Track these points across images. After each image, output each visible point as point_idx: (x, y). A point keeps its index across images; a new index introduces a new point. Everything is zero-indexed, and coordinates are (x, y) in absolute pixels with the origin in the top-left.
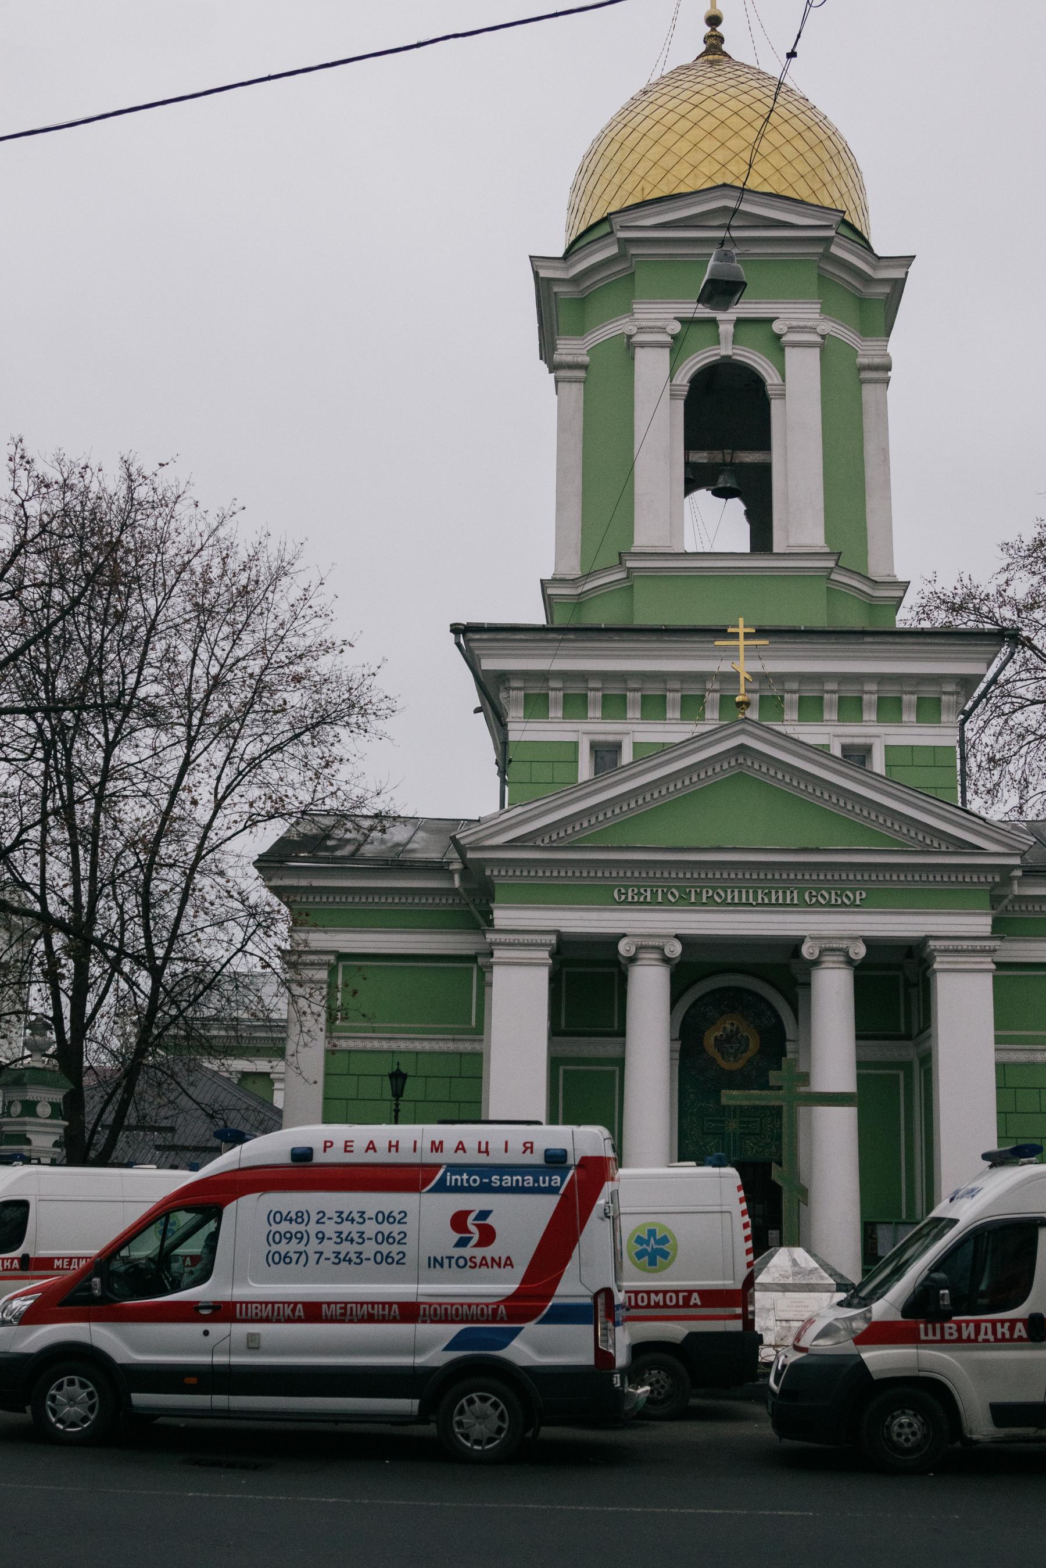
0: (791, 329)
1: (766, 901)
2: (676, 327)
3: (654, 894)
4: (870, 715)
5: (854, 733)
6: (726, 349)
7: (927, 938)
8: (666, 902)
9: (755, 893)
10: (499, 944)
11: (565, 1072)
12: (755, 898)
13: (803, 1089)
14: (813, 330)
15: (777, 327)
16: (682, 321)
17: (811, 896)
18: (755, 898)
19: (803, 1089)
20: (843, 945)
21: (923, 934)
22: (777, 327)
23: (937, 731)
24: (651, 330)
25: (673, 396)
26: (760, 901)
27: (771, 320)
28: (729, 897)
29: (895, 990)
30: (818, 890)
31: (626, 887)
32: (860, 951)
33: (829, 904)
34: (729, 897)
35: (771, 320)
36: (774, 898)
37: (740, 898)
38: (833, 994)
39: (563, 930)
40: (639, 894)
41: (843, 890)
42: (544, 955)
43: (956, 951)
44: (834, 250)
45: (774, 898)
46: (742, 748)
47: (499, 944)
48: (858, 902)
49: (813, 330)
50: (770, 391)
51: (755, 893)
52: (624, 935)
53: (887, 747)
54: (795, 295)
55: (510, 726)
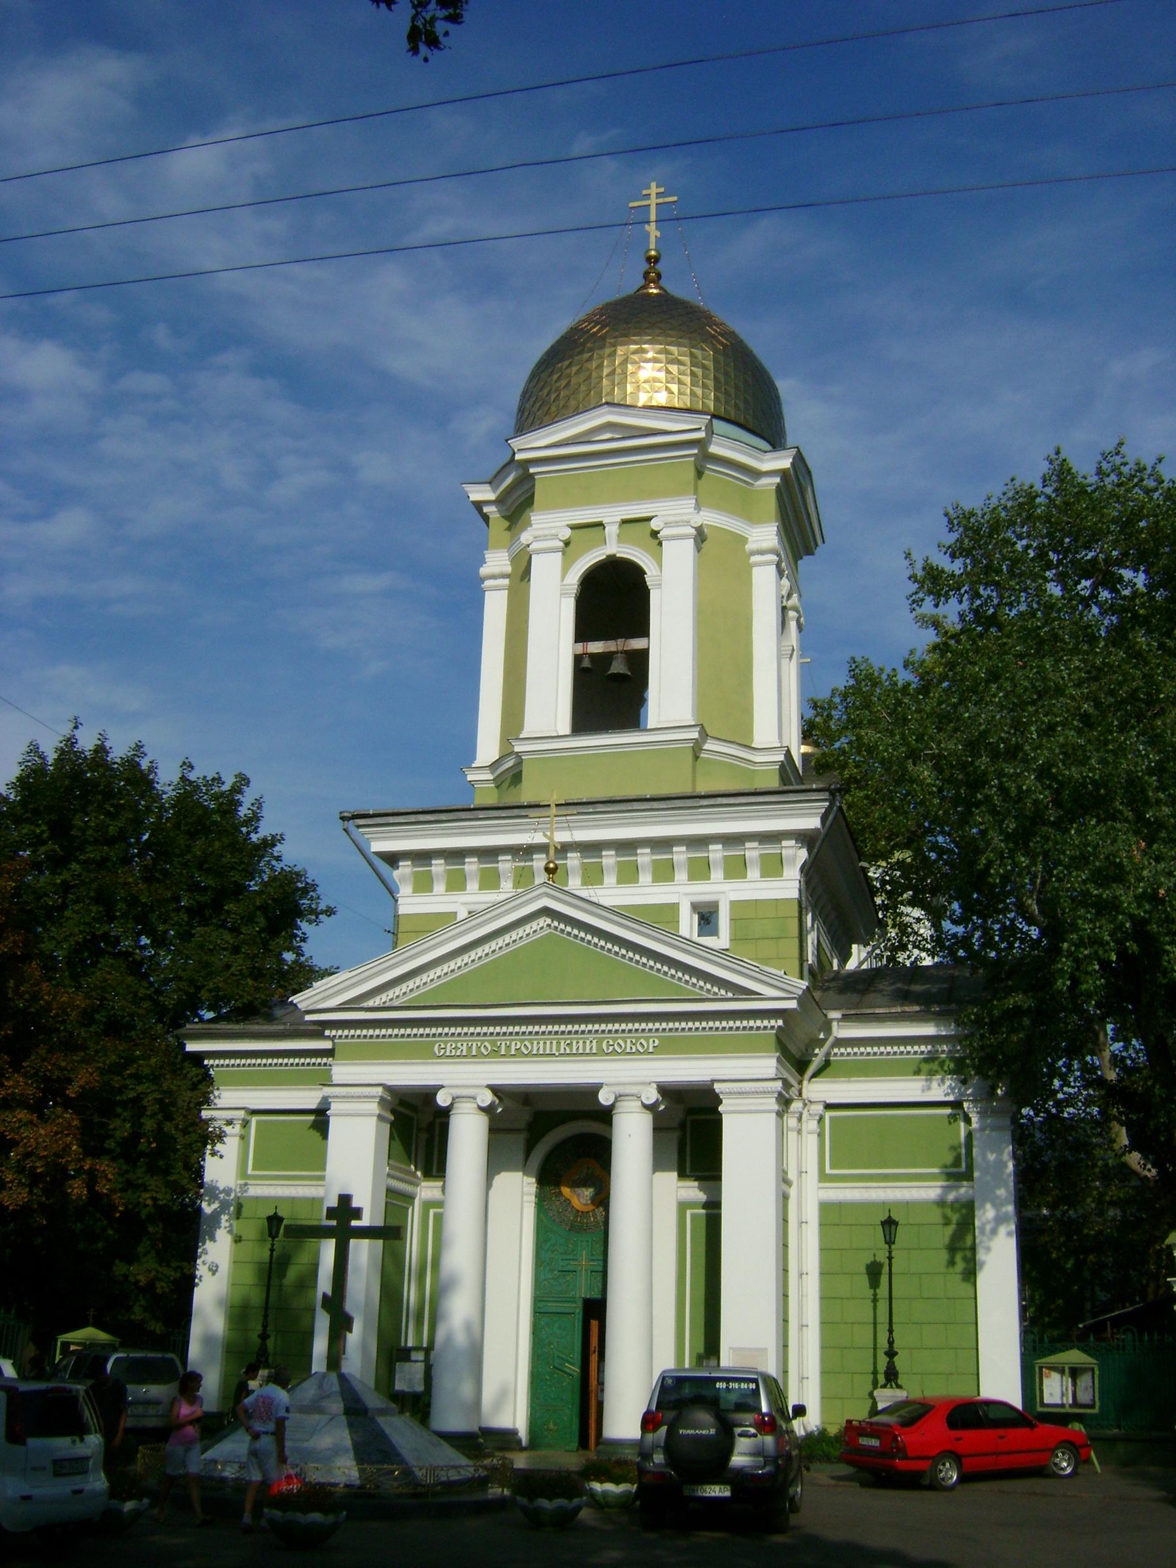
0: (667, 525)
1: (568, 1051)
2: (567, 533)
3: (470, 1048)
4: (717, 874)
5: (704, 891)
6: (613, 547)
7: (713, 1081)
8: (479, 1055)
9: (558, 1043)
10: (337, 1097)
11: (692, 1215)
12: (558, 1049)
13: (354, 1223)
14: (687, 523)
15: (654, 525)
16: (573, 527)
17: (609, 1045)
18: (558, 1049)
19: (354, 1223)
20: (634, 1090)
21: (708, 1078)
22: (654, 525)
23: (746, 885)
24: (545, 538)
25: (563, 594)
26: (562, 1051)
27: (649, 519)
28: (535, 1049)
29: (691, 1131)
30: (615, 1039)
31: (446, 1043)
32: (652, 1096)
33: (625, 1053)
34: (535, 1049)
35: (649, 519)
36: (575, 1048)
37: (584, 1049)
38: (632, 1138)
39: (390, 1083)
40: (456, 1048)
41: (638, 1039)
42: (374, 1107)
43: (742, 1094)
44: (714, 449)
45: (575, 1048)
46: (546, 911)
47: (337, 1097)
48: (651, 1050)
49: (687, 523)
50: (649, 580)
51: (558, 1043)
52: (443, 1087)
53: (734, 904)
54: (676, 492)
55: (400, 901)
